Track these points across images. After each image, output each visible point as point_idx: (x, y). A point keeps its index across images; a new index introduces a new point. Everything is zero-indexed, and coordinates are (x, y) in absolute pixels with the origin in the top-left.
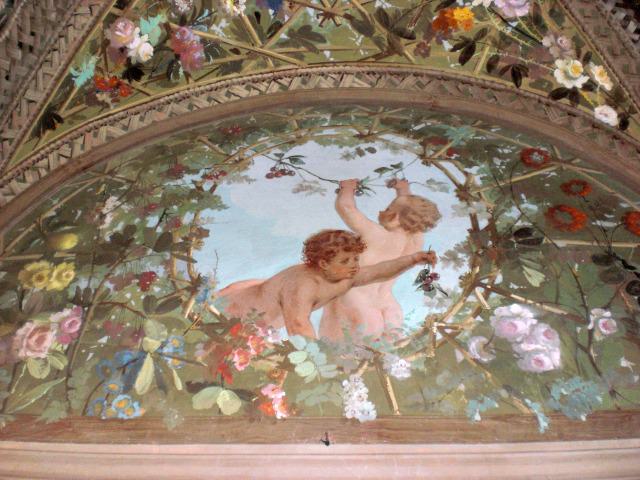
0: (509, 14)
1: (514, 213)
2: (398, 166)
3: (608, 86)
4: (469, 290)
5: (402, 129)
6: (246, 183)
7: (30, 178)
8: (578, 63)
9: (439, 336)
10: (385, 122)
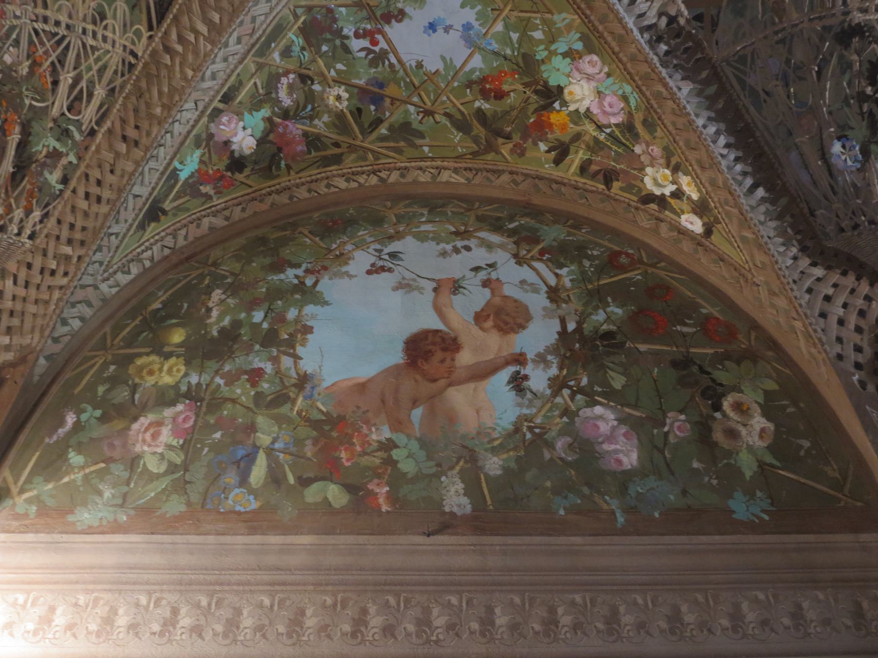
0: (603, 120)
1: (600, 316)
2: (492, 266)
3: (695, 196)
4: (556, 393)
5: (497, 227)
6: (347, 279)
7: (135, 270)
8: (667, 172)
9: (529, 436)
10: (480, 219)
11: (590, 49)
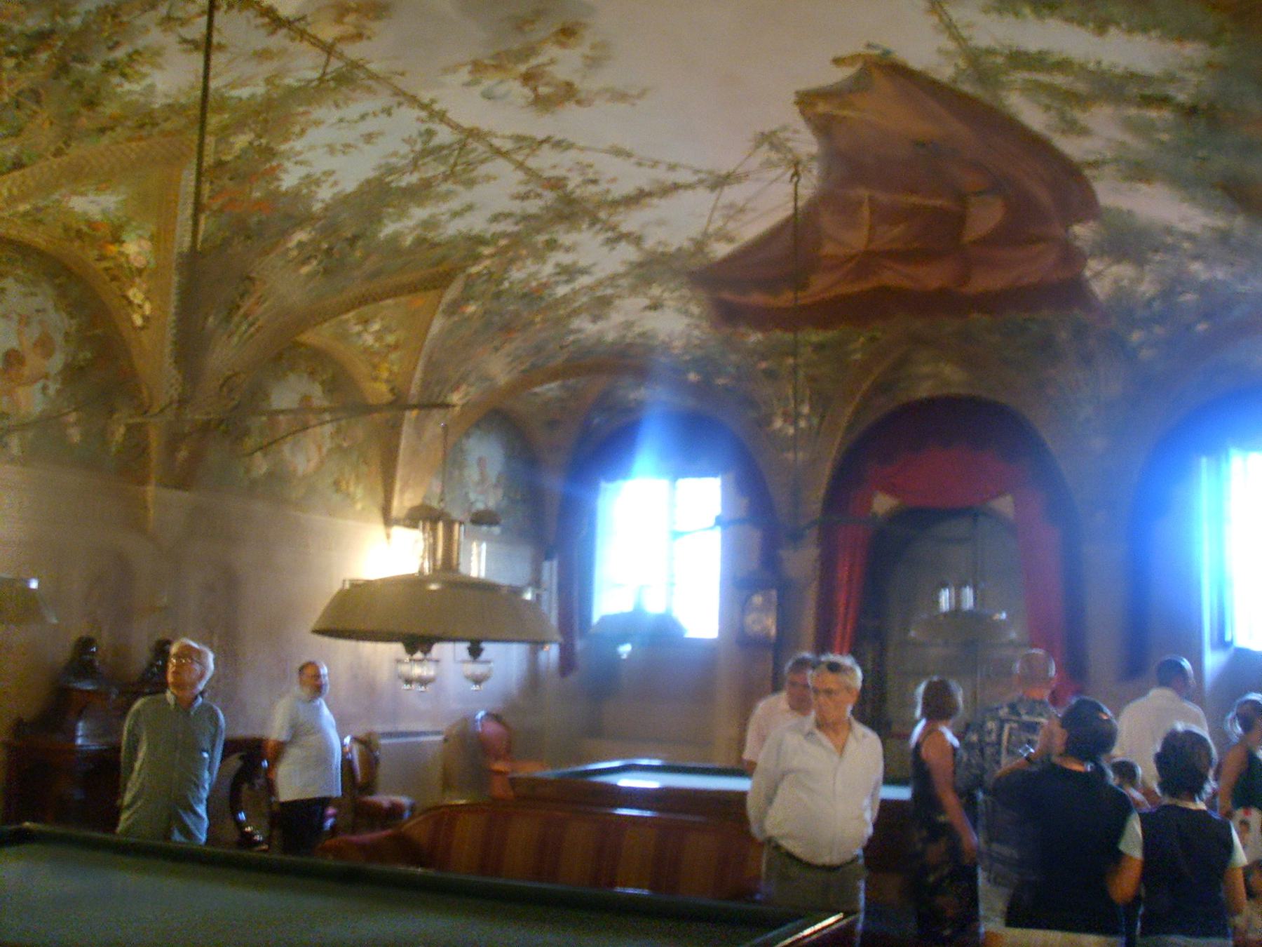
11: (151, 238)
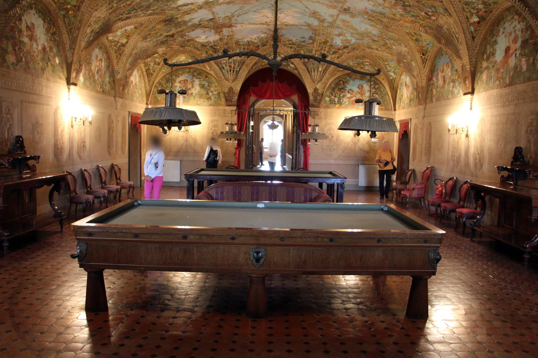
7: (478, 46)
